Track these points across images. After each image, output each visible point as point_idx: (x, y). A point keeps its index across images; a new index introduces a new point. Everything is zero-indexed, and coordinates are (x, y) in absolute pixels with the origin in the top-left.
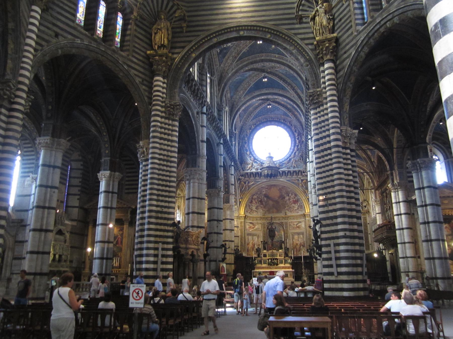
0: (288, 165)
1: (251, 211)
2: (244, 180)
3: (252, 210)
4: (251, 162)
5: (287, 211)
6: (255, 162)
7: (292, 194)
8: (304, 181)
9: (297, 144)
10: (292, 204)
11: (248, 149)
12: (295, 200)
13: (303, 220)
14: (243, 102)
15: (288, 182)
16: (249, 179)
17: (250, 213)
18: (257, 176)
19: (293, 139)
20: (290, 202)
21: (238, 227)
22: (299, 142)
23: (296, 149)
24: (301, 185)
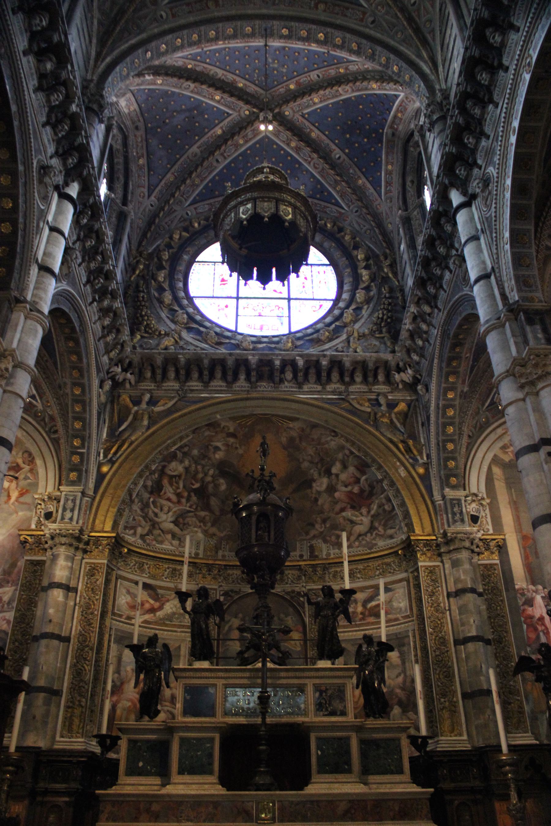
0: (327, 346)
1: (150, 533)
2: (133, 393)
3: (154, 525)
4: (173, 326)
5: (319, 543)
6: (189, 329)
7: (345, 467)
8: (396, 410)
9: (362, 285)
10: (343, 510)
11: (166, 286)
12: (356, 490)
13: (404, 575)
14: (166, 27)
15: (327, 406)
16: (159, 387)
17: (142, 537)
18: (195, 375)
19: (348, 270)
20: (336, 502)
21: (75, 590)
22: (373, 279)
23: (360, 296)
24: (385, 420)
